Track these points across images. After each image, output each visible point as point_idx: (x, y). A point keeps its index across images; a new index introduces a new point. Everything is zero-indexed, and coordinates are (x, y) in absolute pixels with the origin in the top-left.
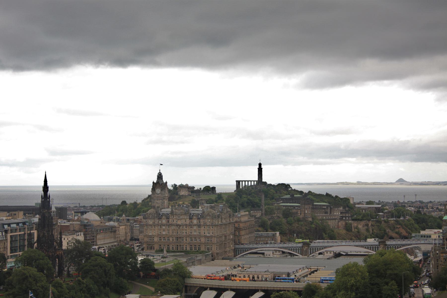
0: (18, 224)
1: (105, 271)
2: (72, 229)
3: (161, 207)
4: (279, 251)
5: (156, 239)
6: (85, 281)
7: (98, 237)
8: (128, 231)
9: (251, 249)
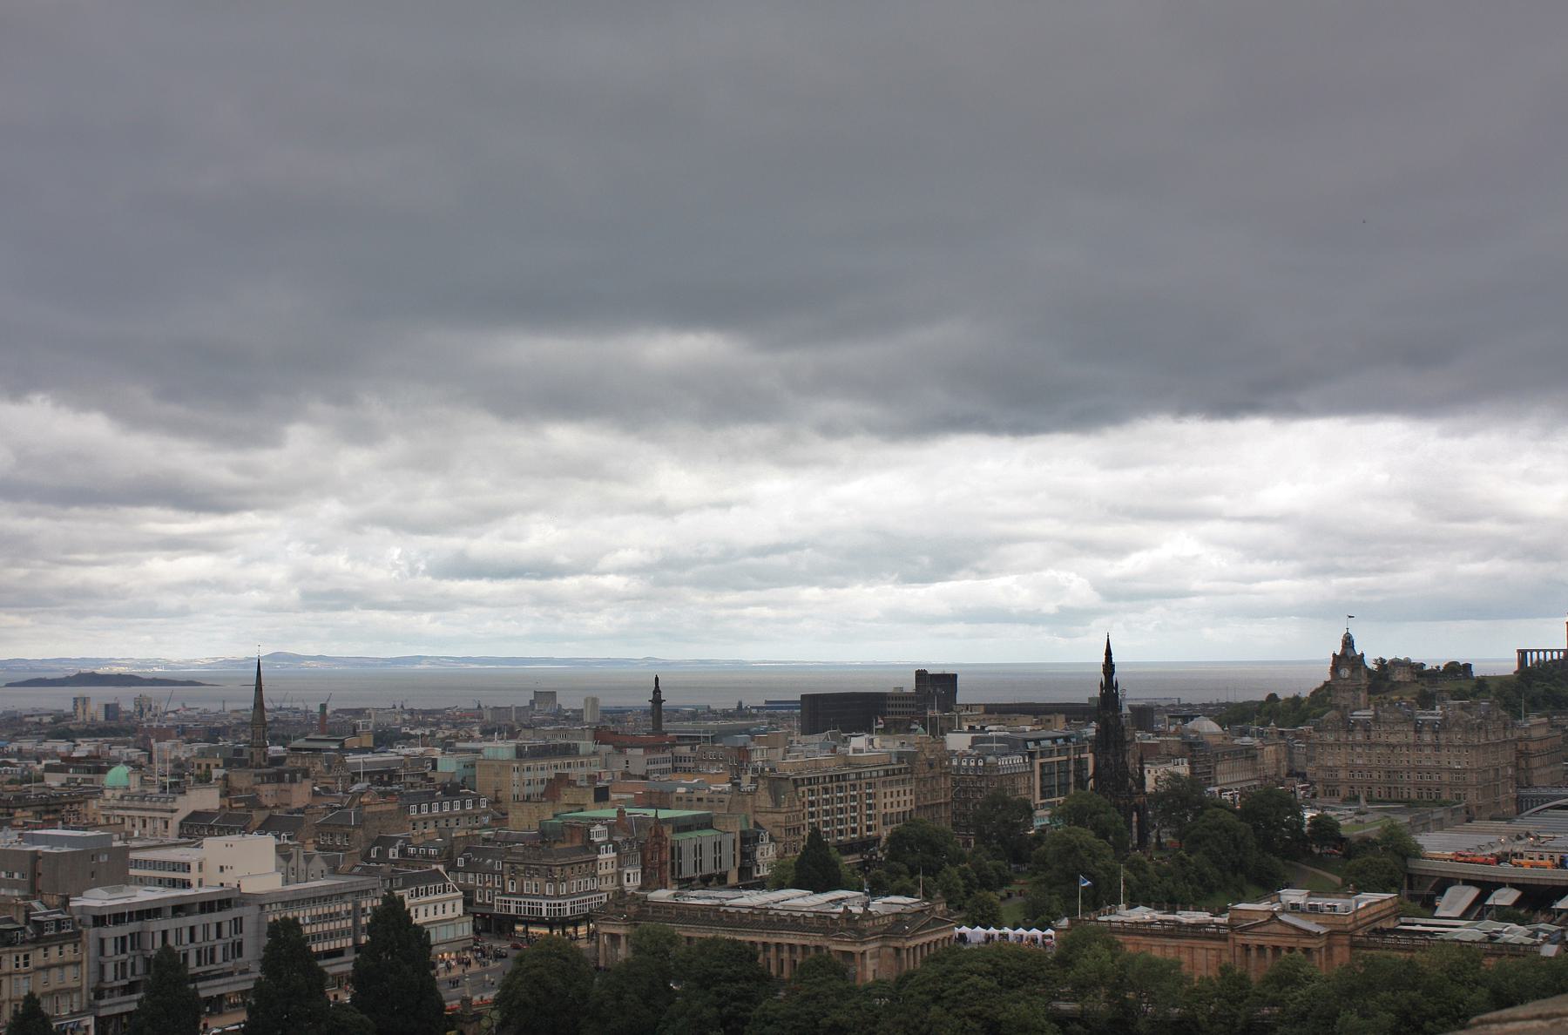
0: (1054, 740)
2: (1164, 751)
6: (1192, 859)
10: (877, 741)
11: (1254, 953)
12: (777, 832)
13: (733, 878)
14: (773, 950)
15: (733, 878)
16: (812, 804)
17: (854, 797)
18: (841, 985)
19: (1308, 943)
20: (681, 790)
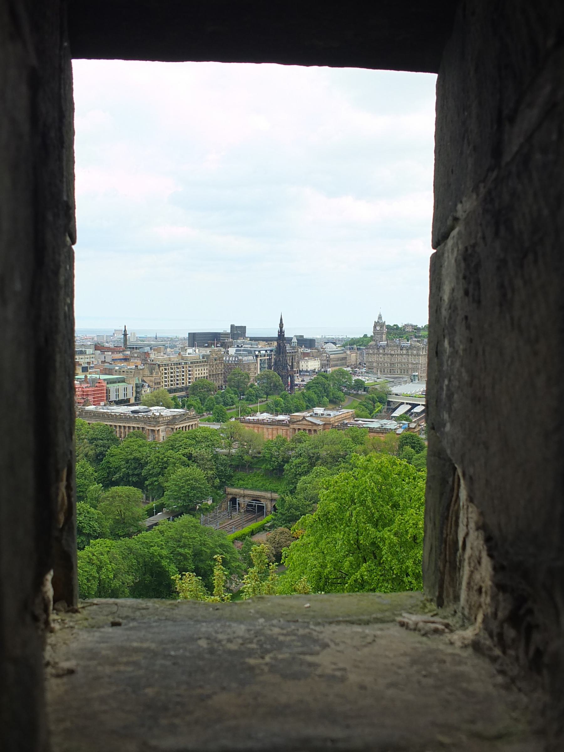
0: (266, 351)
5: (375, 364)
10: (197, 350)
12: (151, 384)
13: (132, 401)
14: (127, 428)
15: (132, 401)
16: (166, 373)
17: (183, 372)
18: (140, 442)
19: (315, 428)
20: (117, 368)
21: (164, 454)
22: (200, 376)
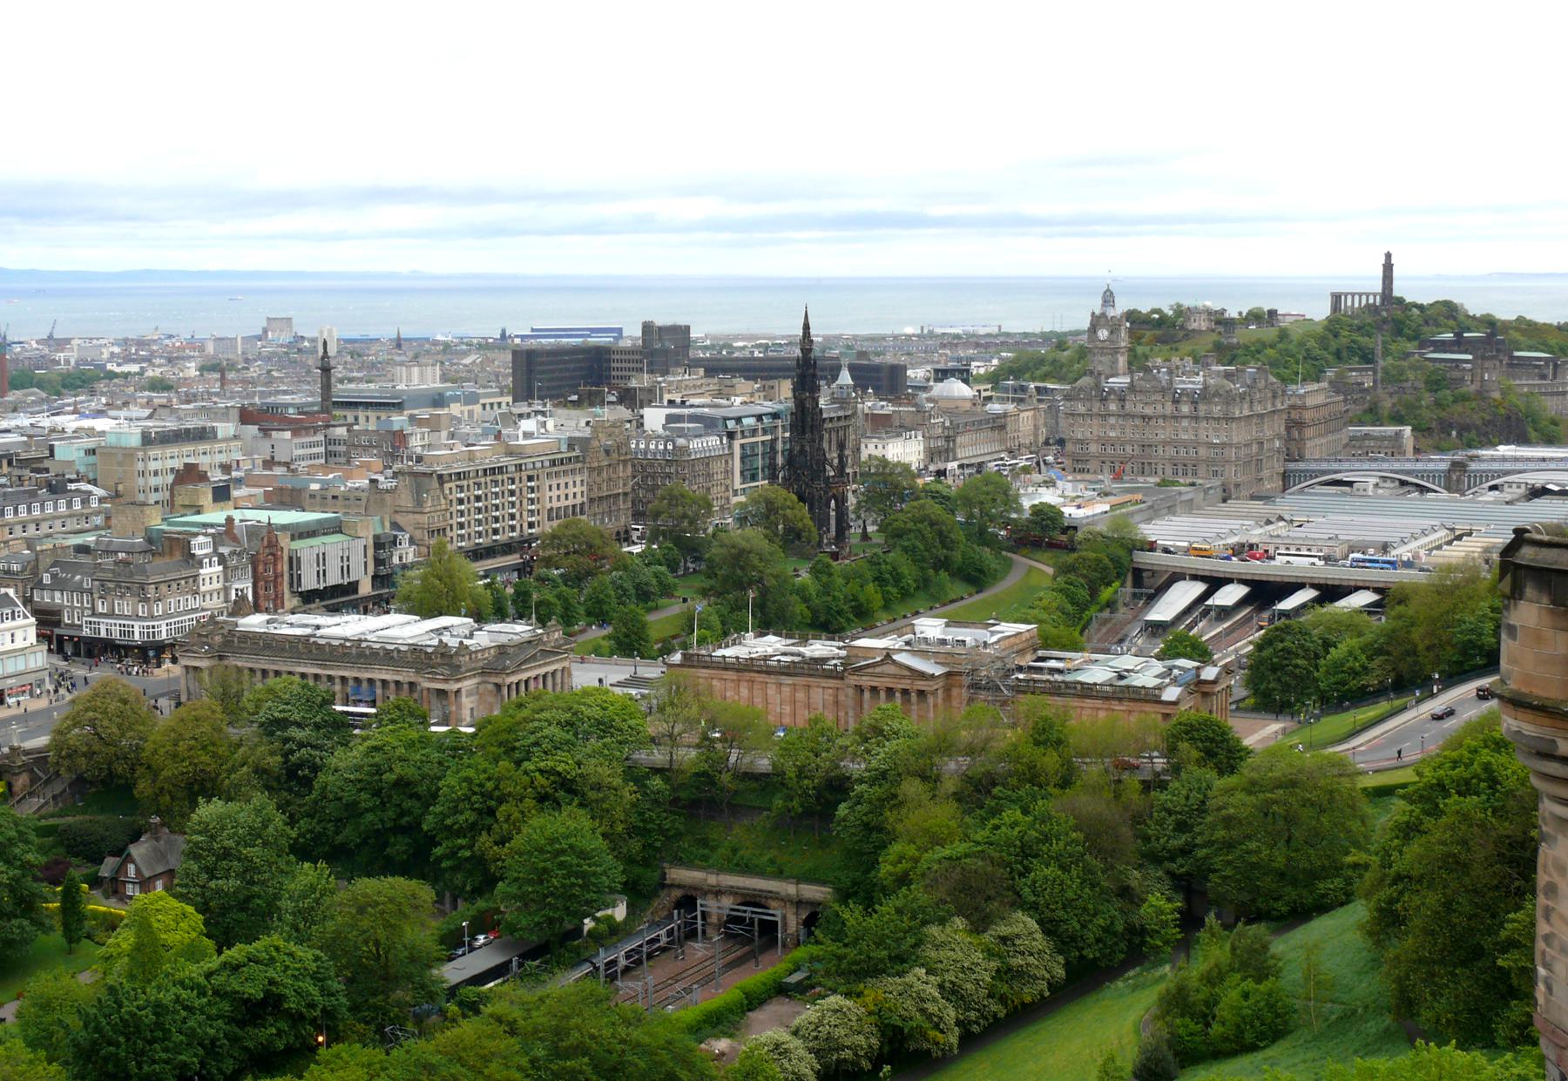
0: (759, 417)
1: (940, 533)
3: (1108, 371)
4: (1393, 480)
7: (958, 440)
8: (1042, 421)
9: (1325, 472)
10: (550, 424)
11: (867, 695)
12: (418, 534)
13: (366, 588)
16: (461, 501)
17: (512, 493)
20: (315, 487)
21: (485, 771)
22: (563, 503)
